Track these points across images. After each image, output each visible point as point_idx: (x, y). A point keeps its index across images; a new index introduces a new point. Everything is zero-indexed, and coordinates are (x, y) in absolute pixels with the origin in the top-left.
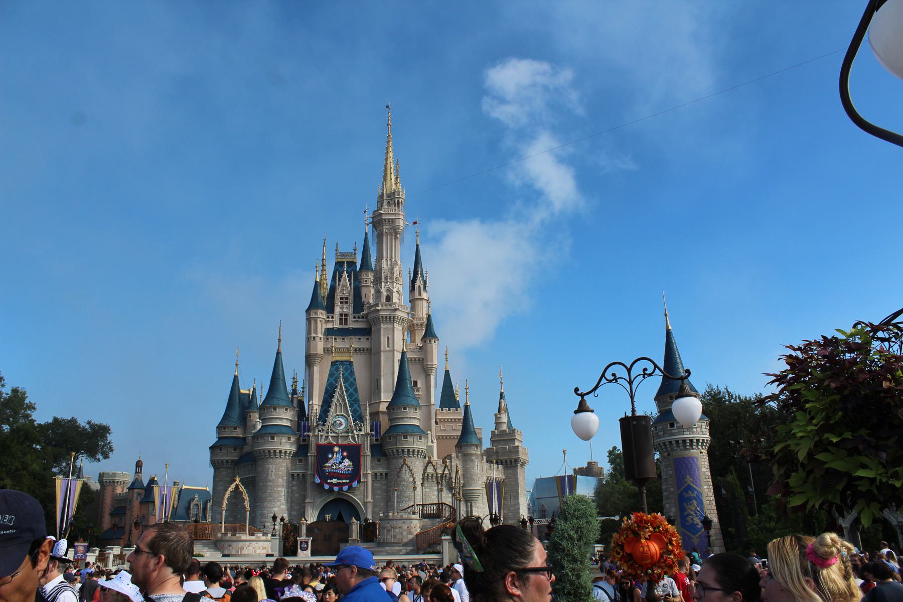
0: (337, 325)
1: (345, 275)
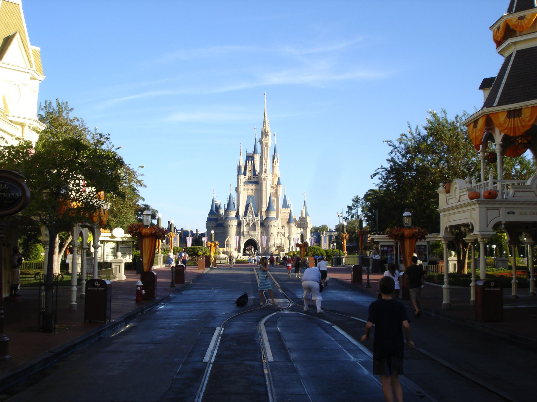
1: (250, 162)
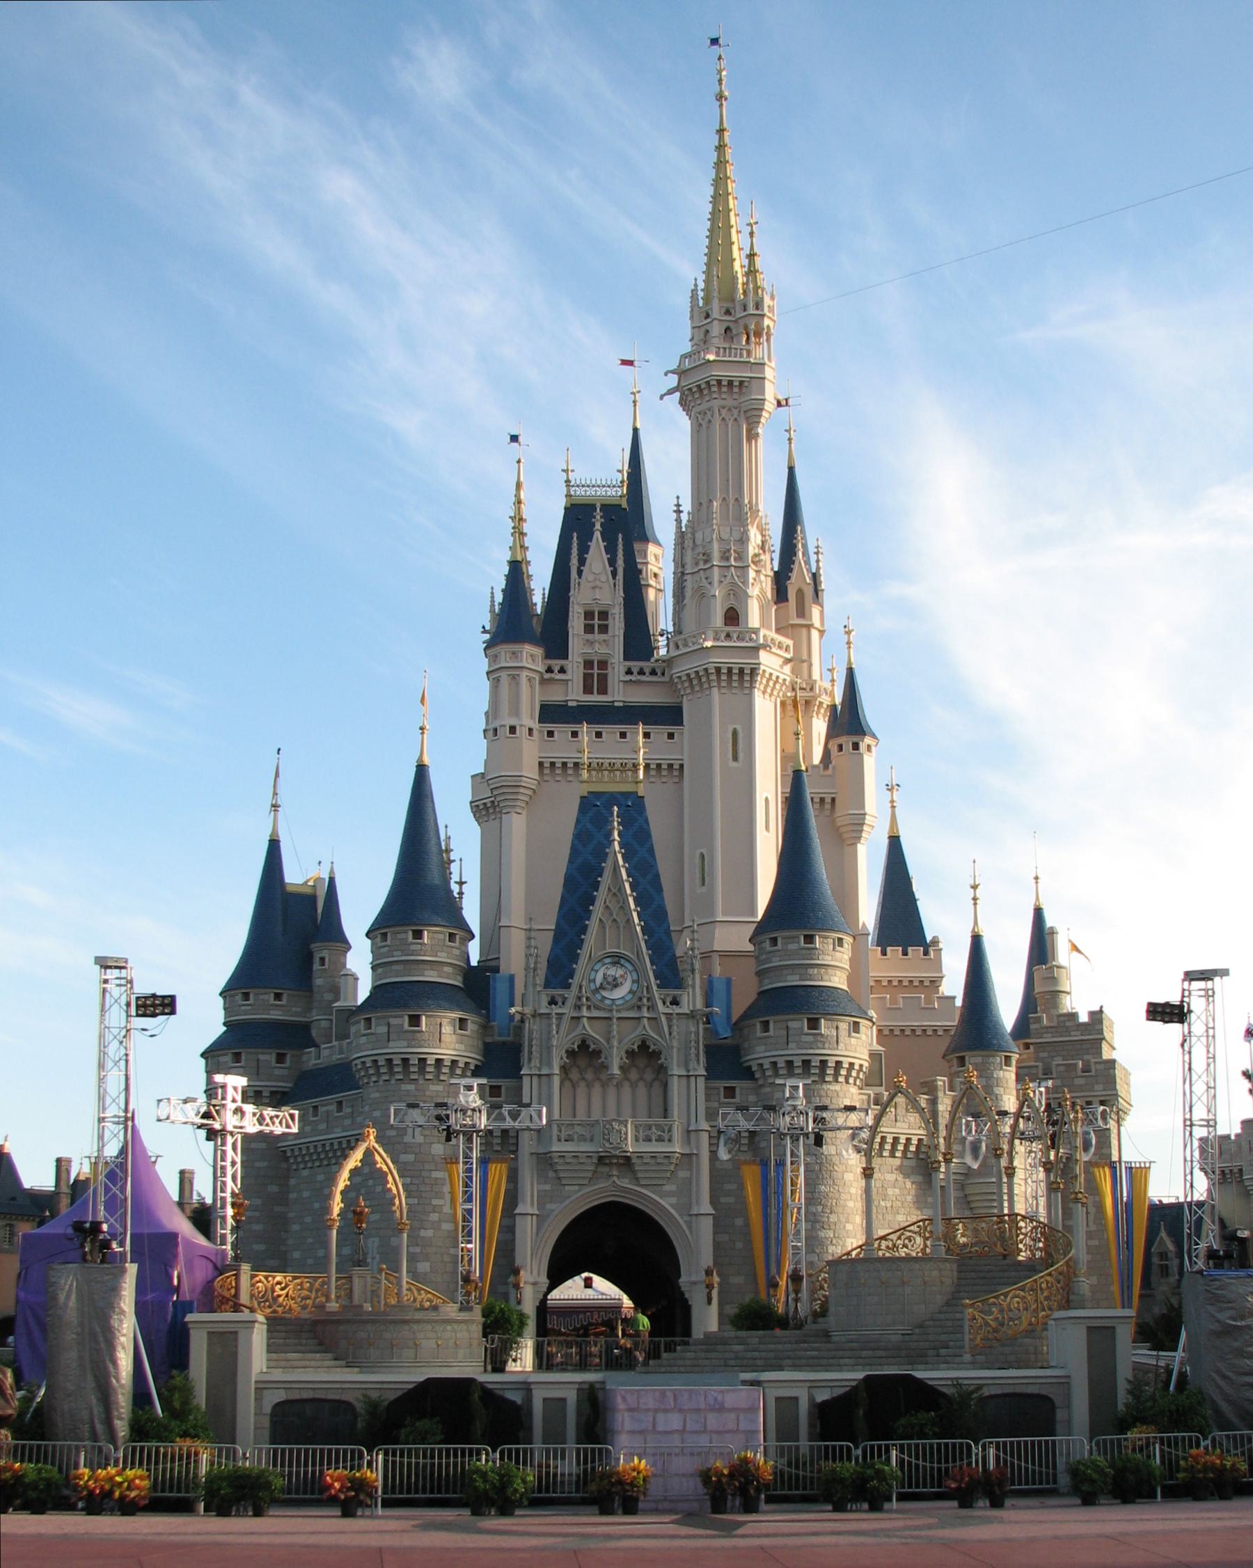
0: (575, 695)
